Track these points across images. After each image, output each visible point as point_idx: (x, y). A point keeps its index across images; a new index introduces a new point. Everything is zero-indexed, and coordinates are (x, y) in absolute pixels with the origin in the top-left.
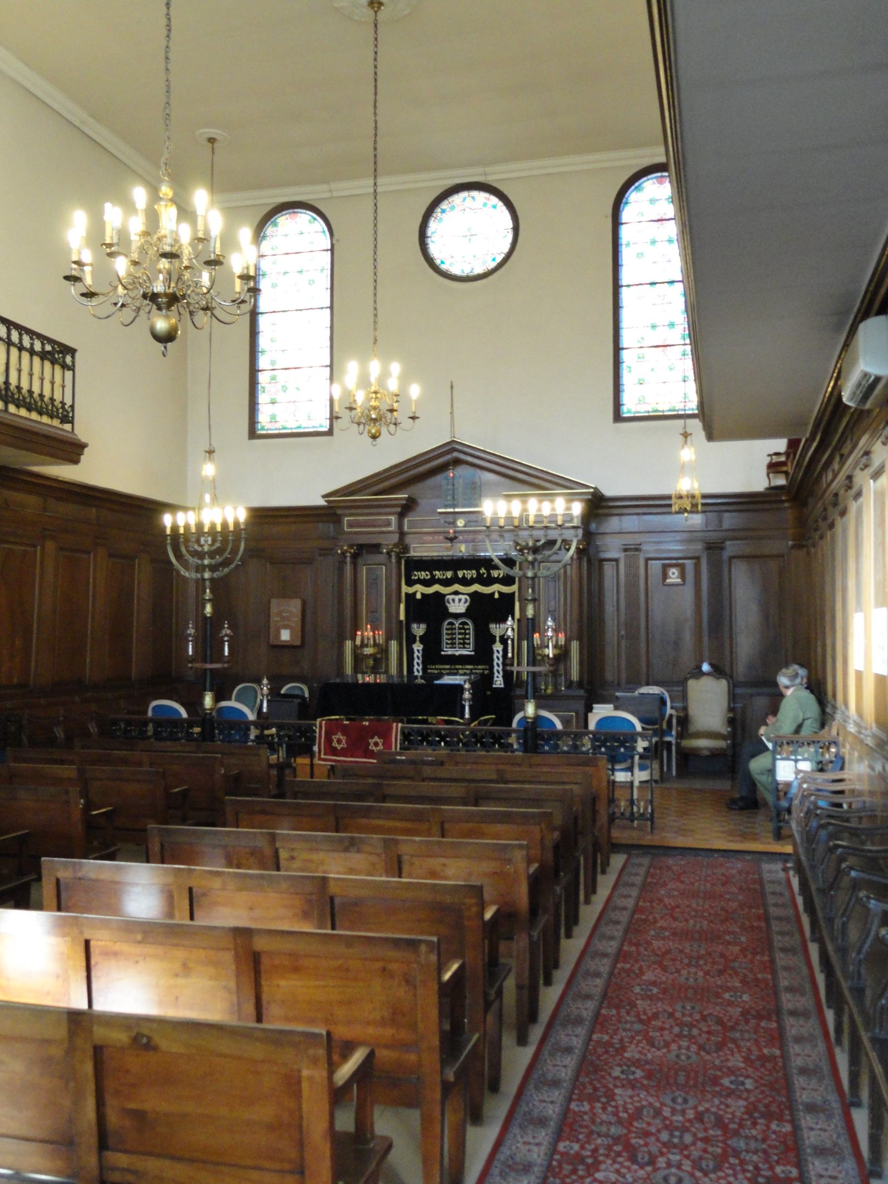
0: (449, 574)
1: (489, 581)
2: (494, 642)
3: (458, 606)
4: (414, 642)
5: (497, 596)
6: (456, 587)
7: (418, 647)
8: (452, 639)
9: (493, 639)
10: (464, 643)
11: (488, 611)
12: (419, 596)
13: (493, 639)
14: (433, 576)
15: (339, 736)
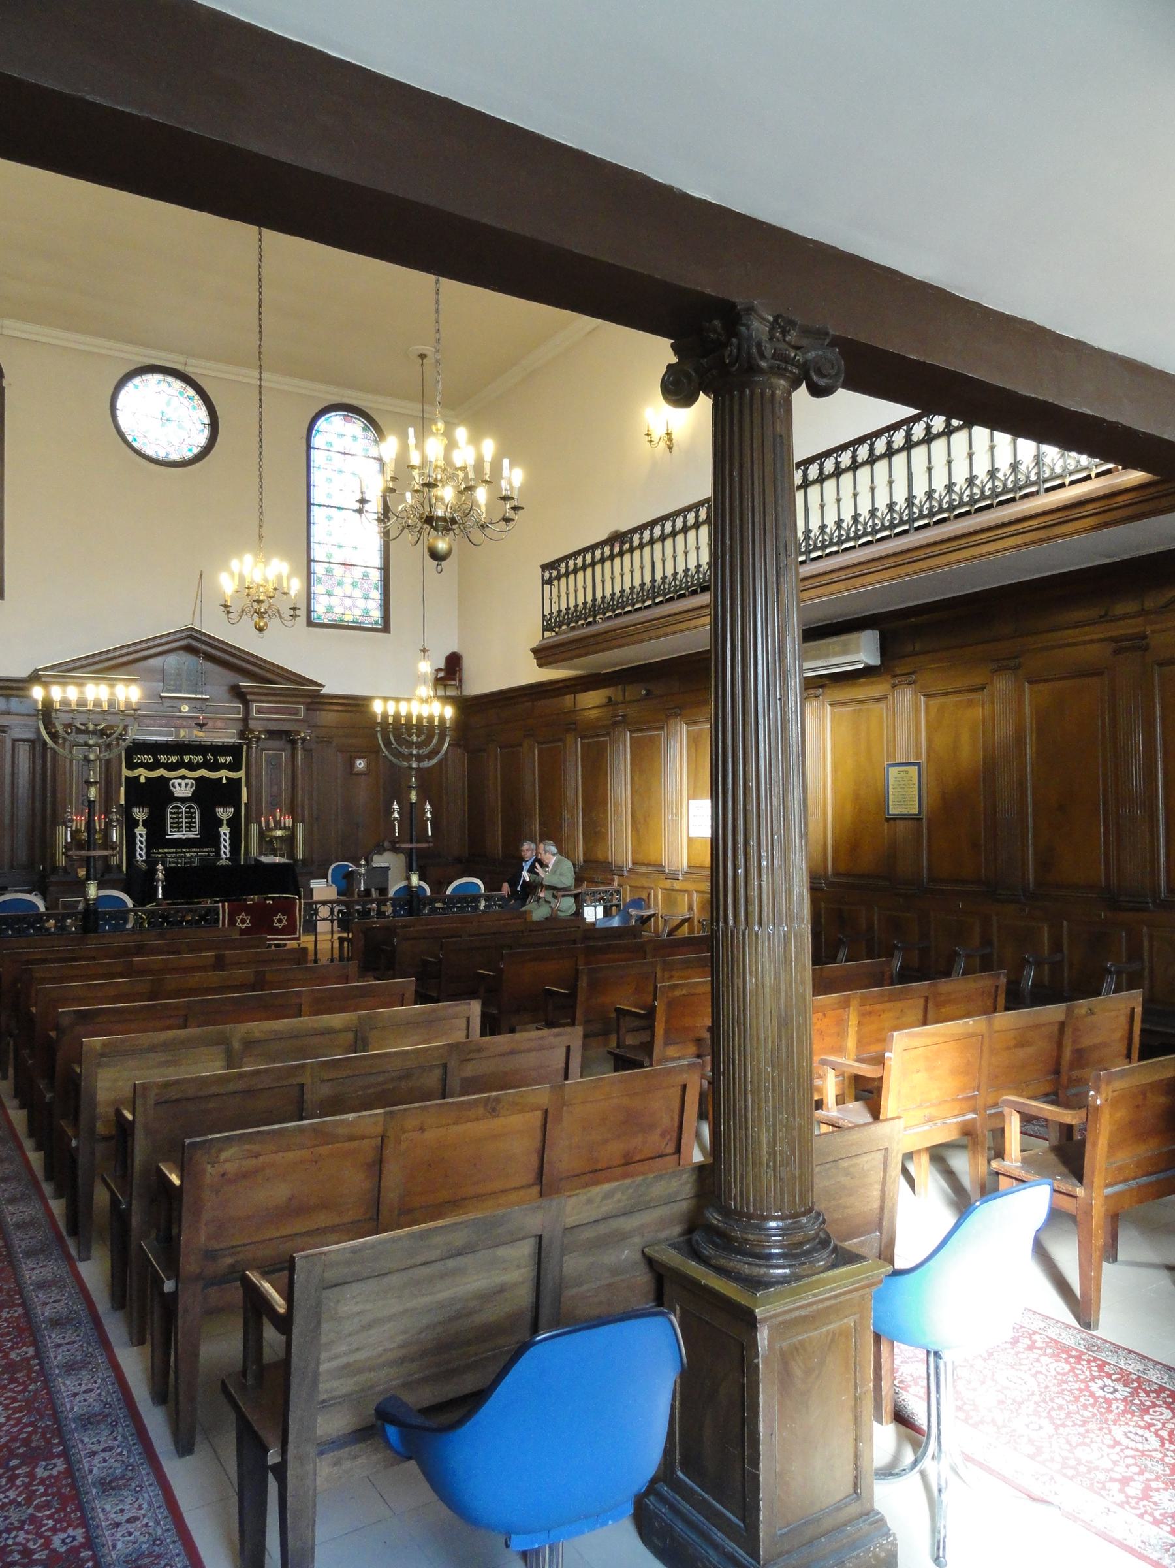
0: (174, 759)
1: (216, 767)
2: (221, 825)
3: (182, 789)
4: (137, 826)
5: (224, 781)
6: (183, 771)
7: (141, 831)
8: (178, 823)
9: (219, 823)
10: (190, 827)
11: (210, 795)
12: (142, 780)
13: (219, 823)
14: (157, 761)
15: (243, 915)
